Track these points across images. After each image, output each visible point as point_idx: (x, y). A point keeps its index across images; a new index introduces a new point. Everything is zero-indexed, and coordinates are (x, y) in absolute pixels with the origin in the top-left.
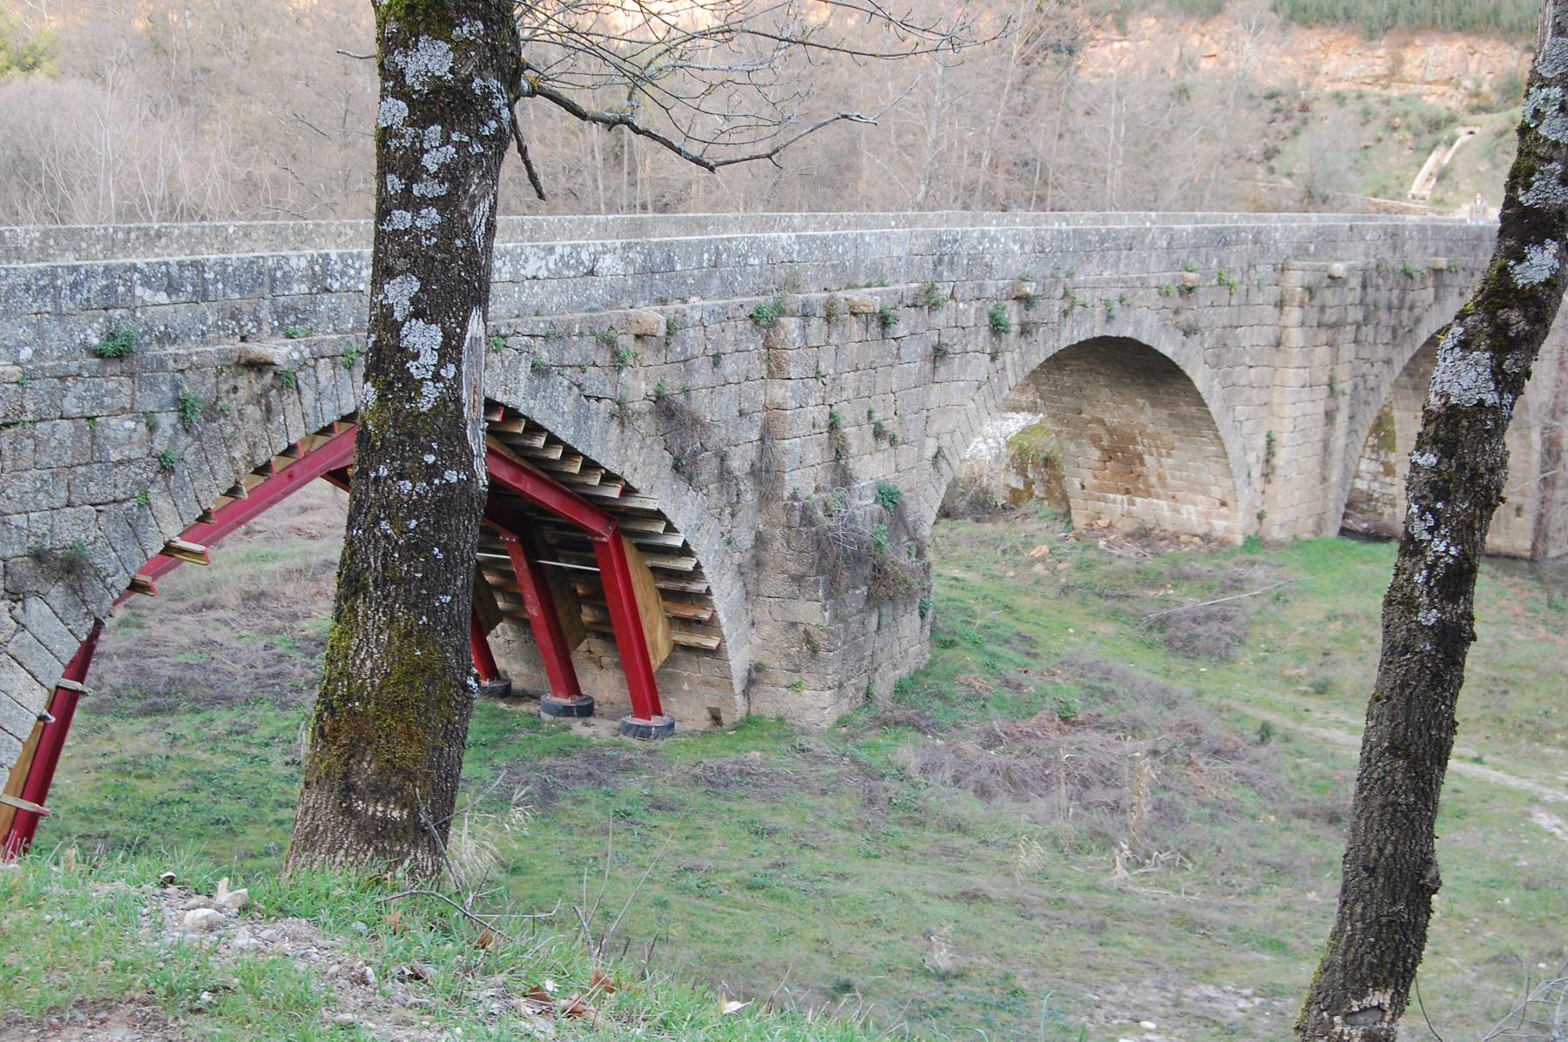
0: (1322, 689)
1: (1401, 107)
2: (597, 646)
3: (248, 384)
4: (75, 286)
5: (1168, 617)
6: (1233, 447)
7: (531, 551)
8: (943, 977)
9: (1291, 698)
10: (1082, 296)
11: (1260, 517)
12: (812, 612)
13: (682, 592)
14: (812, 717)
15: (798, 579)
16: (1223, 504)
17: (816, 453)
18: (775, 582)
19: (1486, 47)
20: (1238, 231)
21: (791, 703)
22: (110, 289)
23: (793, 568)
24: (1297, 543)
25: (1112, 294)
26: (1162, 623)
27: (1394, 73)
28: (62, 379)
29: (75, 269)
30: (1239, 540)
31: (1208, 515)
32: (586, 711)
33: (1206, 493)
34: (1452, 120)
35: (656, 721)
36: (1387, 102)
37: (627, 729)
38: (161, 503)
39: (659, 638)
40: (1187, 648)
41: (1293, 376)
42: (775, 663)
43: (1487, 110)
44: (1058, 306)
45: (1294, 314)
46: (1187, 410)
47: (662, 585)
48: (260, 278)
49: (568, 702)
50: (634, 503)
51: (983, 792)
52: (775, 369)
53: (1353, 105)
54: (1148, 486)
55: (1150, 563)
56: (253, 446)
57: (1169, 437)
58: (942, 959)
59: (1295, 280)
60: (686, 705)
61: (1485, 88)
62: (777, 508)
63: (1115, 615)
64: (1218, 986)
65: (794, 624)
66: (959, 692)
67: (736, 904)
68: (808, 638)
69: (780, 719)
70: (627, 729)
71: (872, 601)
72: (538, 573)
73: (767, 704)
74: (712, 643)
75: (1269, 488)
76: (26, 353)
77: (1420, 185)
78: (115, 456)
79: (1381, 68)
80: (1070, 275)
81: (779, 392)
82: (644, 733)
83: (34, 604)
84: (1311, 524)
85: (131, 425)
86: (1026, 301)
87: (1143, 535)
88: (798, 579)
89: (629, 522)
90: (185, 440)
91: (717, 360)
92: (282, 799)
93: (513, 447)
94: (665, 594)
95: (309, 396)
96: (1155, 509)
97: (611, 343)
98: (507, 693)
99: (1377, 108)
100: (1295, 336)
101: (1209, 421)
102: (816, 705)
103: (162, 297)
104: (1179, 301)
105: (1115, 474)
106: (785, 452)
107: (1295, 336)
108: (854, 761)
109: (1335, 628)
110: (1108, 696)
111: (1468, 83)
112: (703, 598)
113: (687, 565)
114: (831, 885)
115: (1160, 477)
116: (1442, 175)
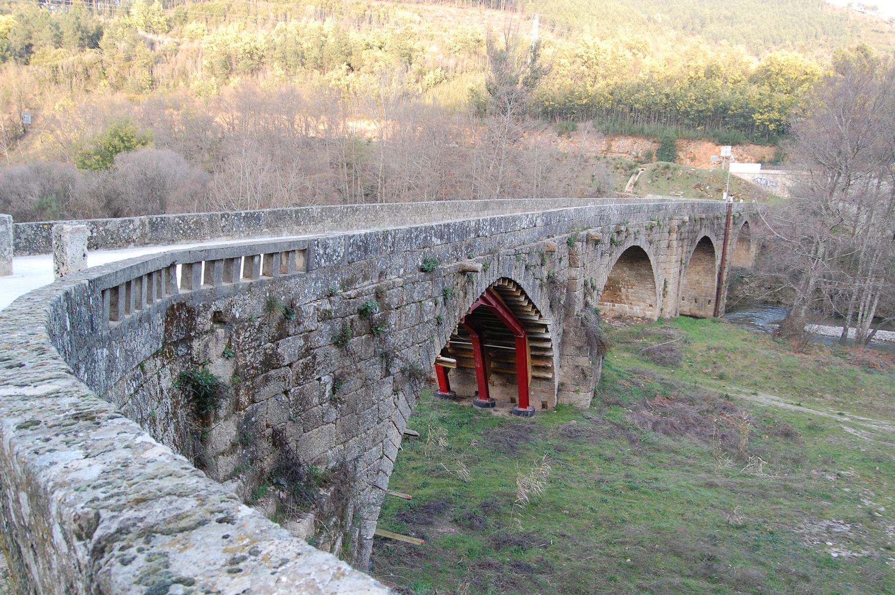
0: (721, 377)
2: (493, 378)
3: (462, 280)
4: (417, 236)
5: (649, 350)
6: (657, 285)
7: (482, 341)
8: (738, 528)
9: (713, 381)
10: (631, 230)
11: (662, 310)
12: (584, 361)
13: (542, 355)
14: (583, 403)
15: (579, 348)
16: (651, 306)
17: (581, 297)
18: (570, 350)
19: (639, 141)
20: (662, 205)
21: (574, 398)
22: (426, 237)
23: (578, 344)
24: (671, 319)
25: (635, 230)
26: (648, 352)
27: (609, 149)
28: (413, 283)
29: (417, 229)
30: (656, 319)
31: (644, 310)
32: (493, 405)
33: (644, 302)
34: (636, 166)
35: (529, 409)
36: (614, 159)
37: (519, 413)
38: (436, 340)
39: (530, 373)
40: (661, 362)
41: (674, 258)
42: (568, 382)
43: (642, 163)
44: (625, 234)
45: (674, 236)
46: (643, 272)
47: (533, 353)
48: (463, 231)
49: (487, 401)
50: (541, 322)
51: (666, 433)
52: (572, 264)
53: (603, 160)
54: (621, 299)
55: (629, 329)
56: (461, 309)
57: (634, 281)
58: (739, 520)
59: (675, 223)
60: (535, 403)
61: (640, 155)
62: (571, 320)
63: (627, 350)
64: (831, 520)
65: (577, 366)
66: (621, 388)
67: (631, 498)
68: (583, 372)
69: (571, 405)
70: (519, 413)
71: (598, 353)
72: (482, 348)
73: (565, 400)
74: (550, 376)
75: (665, 300)
76: (402, 270)
77: (628, 188)
78: (426, 320)
79: (604, 148)
80: (627, 223)
81: (574, 272)
82: (526, 414)
83: (401, 395)
84: (674, 312)
85: (431, 303)
86: (619, 233)
87: (619, 318)
88: (579, 348)
89: (532, 329)
90: (444, 309)
91: (561, 259)
92: (407, 456)
93: (505, 301)
94: (533, 357)
95: (475, 284)
96: (624, 308)
97: (543, 255)
98: (456, 398)
99: (611, 161)
100: (675, 243)
101: (652, 276)
102: (584, 398)
103: (439, 242)
104: (649, 232)
105: (608, 295)
106: (576, 297)
107: (675, 243)
108: (611, 423)
109: (712, 352)
110: (672, 387)
111: (634, 153)
112: (549, 358)
113: (548, 345)
114: (655, 484)
115: (627, 296)
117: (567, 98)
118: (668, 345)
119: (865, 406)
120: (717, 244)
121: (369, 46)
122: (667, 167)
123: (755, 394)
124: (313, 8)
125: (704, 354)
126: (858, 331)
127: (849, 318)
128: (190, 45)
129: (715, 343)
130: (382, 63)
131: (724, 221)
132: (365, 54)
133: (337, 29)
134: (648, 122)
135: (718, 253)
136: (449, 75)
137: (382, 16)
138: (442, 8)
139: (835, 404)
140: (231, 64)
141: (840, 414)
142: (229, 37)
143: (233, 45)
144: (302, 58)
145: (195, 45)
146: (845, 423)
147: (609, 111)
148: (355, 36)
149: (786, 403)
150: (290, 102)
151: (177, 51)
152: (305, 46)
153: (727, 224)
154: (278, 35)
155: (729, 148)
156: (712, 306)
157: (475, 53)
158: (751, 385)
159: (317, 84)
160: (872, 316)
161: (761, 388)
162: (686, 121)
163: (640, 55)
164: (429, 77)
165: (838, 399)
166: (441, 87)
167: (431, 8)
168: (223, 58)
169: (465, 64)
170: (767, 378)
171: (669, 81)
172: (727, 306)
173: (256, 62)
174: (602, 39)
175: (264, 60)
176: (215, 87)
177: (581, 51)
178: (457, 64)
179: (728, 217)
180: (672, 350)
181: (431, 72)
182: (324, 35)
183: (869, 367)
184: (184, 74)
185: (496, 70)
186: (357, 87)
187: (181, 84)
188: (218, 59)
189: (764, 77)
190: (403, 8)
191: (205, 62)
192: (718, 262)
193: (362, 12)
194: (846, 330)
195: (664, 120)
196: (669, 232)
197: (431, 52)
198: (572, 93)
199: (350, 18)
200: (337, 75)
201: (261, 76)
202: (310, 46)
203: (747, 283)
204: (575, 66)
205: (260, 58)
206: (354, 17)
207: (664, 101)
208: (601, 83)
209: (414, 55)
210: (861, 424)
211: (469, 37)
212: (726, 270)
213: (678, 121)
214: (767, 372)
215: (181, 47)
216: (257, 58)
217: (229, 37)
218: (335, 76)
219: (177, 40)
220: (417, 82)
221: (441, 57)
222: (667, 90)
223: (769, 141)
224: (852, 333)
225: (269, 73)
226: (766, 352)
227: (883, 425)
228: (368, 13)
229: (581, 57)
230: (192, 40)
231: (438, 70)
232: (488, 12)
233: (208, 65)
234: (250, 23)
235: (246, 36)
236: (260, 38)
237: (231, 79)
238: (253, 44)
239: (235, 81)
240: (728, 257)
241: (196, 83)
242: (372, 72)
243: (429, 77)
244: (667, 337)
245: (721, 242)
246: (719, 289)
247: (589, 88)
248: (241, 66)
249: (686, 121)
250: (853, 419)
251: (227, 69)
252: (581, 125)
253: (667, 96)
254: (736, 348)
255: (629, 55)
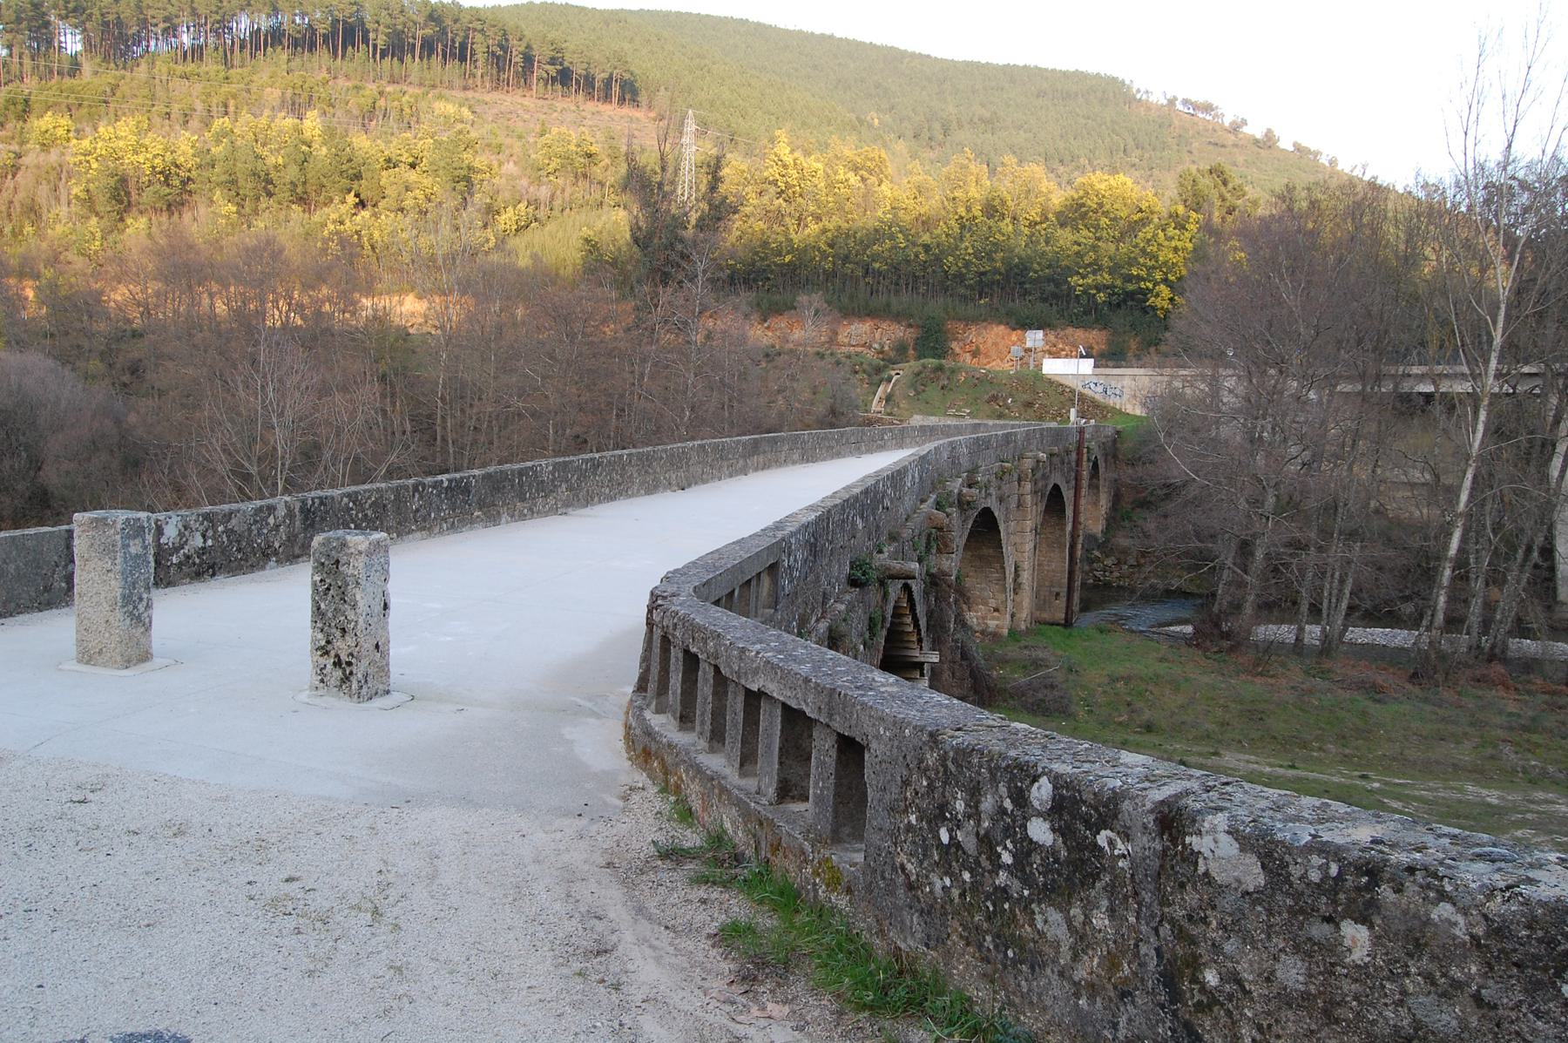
1: (859, 359)
11: (1013, 616)
16: (996, 610)
24: (1028, 631)
27: (832, 341)
30: (1005, 632)
33: (986, 604)
34: (886, 367)
36: (849, 357)
41: (1029, 524)
45: (1028, 487)
46: (985, 551)
53: (828, 359)
59: (1028, 464)
75: (1018, 598)
77: (876, 406)
101: (1000, 557)
116: (889, 399)
117: (756, 253)
118: (1046, 677)
119: (1394, 759)
120: (1068, 495)
121: (390, 163)
122: (940, 368)
123: (1216, 754)
124: (277, 93)
125: (1108, 689)
126: (1324, 630)
127: (1304, 608)
128: (42, 156)
129: (1121, 670)
130: (419, 194)
131: (1074, 456)
132: (386, 178)
133: (330, 133)
134: (897, 292)
135: (1069, 512)
136: (541, 214)
137: (407, 110)
138: (508, 98)
139: (1346, 759)
140: (128, 194)
141: (1364, 777)
142: (121, 144)
143: (129, 158)
144: (267, 184)
145: (53, 157)
146: (1378, 791)
147: (830, 276)
148: (362, 143)
149: (1271, 765)
150: (263, 267)
151: (15, 169)
152: (271, 160)
153: (1079, 462)
154: (218, 142)
155: (1040, 334)
156: (1061, 603)
157: (585, 176)
158: (1202, 738)
159: (299, 230)
160: (1344, 605)
161: (1219, 742)
162: (962, 291)
163: (873, 179)
164: (507, 219)
165: (1347, 751)
166: (527, 236)
167: (487, 98)
168: (112, 182)
169: (567, 194)
170: (1224, 724)
171: (926, 223)
172: (1081, 600)
173: (176, 191)
174: (807, 153)
175: (191, 186)
176: (98, 235)
177: (773, 172)
178: (552, 196)
179: (1079, 453)
180: (1052, 687)
181: (510, 209)
182: (304, 143)
183: (1375, 692)
184: (33, 211)
185: (645, 204)
186: (376, 234)
187: (28, 229)
188: (101, 187)
189: (1076, 214)
190: (440, 97)
191: (75, 191)
192: (1069, 527)
193: (370, 101)
194: (1301, 630)
195: (922, 289)
196: (1019, 480)
197: (503, 174)
198: (765, 244)
199: (348, 112)
200: (337, 215)
201: (187, 216)
202: (280, 161)
203: (1098, 560)
204: (765, 199)
205: (184, 183)
206: (356, 112)
207: (922, 257)
208: (814, 228)
209: (476, 178)
210: (1399, 790)
211: (573, 148)
212: (1081, 540)
213: (946, 290)
214: (1219, 712)
215: (25, 160)
216: (177, 183)
217: (121, 144)
218: (334, 216)
219: (16, 147)
220: (485, 226)
221: (525, 182)
222: (926, 238)
223: (1097, 321)
224: (1313, 632)
225: (202, 210)
226: (1206, 679)
227: (1436, 790)
228: (381, 103)
229: (775, 183)
230: (45, 147)
231: (522, 206)
232: (591, 106)
233: (83, 195)
234: (157, 120)
235: (155, 144)
236: (185, 146)
237: (129, 221)
238: (169, 157)
239: (137, 225)
240: (1082, 519)
241: (59, 229)
242: (402, 210)
243: (507, 219)
244: (1037, 664)
245: (1072, 492)
246: (1071, 573)
247: (793, 236)
248: (147, 197)
249: (962, 291)
250: (1386, 783)
251: (121, 202)
252: (803, 298)
253: (927, 248)
254: (1158, 676)
255: (854, 179)
